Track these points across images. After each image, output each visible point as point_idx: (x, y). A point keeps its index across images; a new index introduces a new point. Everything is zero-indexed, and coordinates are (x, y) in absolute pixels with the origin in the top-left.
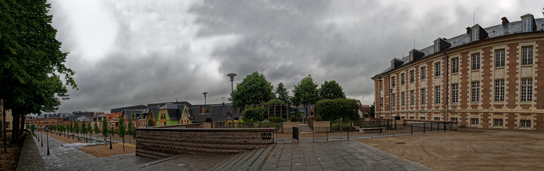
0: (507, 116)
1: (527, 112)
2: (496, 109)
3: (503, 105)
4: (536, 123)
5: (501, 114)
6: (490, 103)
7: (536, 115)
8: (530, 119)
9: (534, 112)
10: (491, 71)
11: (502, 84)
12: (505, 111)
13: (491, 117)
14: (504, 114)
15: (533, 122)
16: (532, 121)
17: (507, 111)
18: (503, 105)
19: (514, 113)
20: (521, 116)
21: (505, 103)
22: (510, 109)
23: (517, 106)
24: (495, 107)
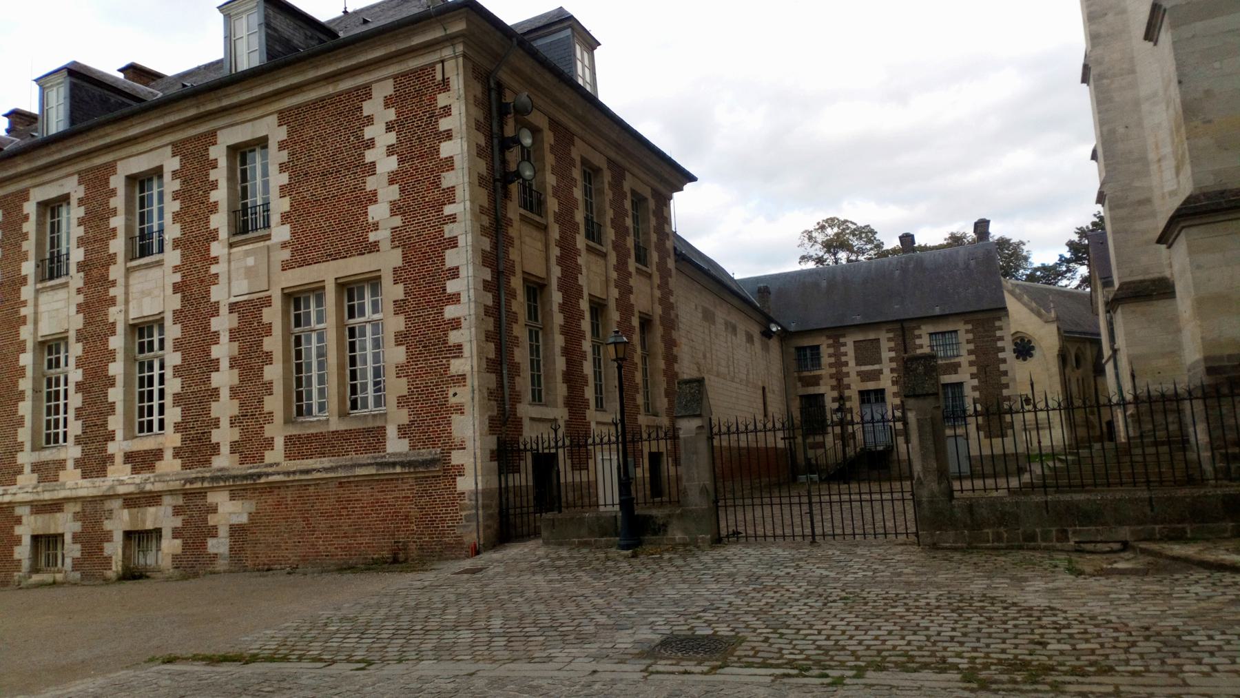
1: (47, 496)
4: (78, 546)
7: (78, 508)
8: (60, 531)
9: (74, 494)
19: (11, 505)
20: (33, 517)
23: (20, 471)
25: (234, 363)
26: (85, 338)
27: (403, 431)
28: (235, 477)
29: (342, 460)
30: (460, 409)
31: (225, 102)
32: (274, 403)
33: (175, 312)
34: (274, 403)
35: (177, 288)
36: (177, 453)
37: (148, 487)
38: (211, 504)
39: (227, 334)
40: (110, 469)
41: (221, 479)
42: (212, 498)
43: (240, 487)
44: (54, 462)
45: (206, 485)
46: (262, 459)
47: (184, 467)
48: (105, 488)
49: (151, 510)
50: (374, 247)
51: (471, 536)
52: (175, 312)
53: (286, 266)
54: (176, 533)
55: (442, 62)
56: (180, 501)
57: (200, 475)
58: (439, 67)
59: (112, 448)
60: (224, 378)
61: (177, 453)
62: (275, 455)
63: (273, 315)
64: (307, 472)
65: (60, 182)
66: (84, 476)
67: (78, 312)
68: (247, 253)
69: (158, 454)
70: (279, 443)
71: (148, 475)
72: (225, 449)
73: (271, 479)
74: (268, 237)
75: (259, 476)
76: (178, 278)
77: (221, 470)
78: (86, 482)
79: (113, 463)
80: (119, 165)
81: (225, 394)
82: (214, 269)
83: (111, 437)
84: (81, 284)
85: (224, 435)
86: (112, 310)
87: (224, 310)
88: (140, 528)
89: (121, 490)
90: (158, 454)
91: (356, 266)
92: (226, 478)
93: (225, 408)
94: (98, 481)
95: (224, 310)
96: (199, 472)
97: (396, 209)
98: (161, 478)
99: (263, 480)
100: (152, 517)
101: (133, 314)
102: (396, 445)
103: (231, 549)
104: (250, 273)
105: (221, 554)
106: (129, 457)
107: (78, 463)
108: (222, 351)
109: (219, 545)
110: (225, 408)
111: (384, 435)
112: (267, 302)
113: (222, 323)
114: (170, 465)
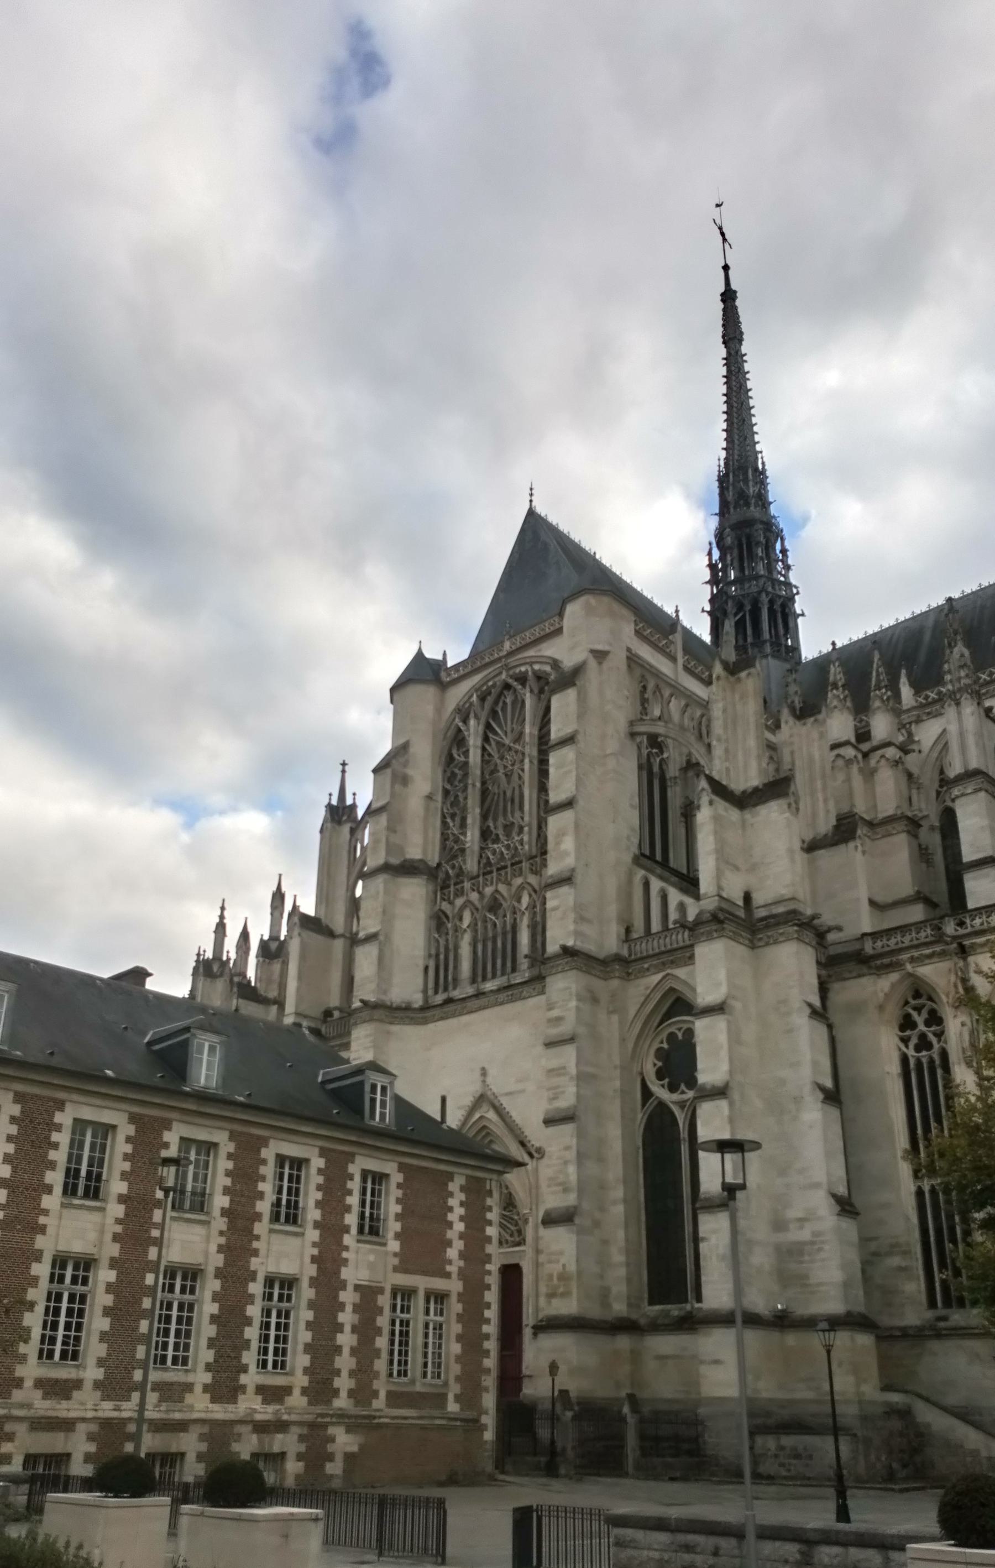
0: (91, 1437)
1: (177, 1416)
2: (48, 1404)
3: (77, 1384)
5: (67, 1425)
6: (20, 1371)
7: (206, 1429)
10: (46, 1212)
11: (74, 1280)
12: (90, 1414)
13: (16, 1443)
14: (82, 1428)
15: (194, 1459)
16: (191, 1457)
17: (100, 1414)
18: (77, 1384)
21: (92, 1373)
22: (108, 1405)
24: (39, 1393)
25: (354, 1329)
26: (225, 1277)
27: (458, 1398)
28: (356, 1417)
29: (424, 1413)
30: (487, 1390)
31: (379, 1144)
32: (381, 1365)
33: (311, 1278)
34: (381, 1365)
35: (314, 1259)
36: (304, 1391)
37: (285, 1417)
38: (330, 1435)
39: (351, 1307)
40: (241, 1397)
41: (341, 1416)
42: (331, 1430)
43: (353, 1424)
44: (179, 1384)
45: (334, 1420)
46: (370, 1404)
47: (310, 1403)
48: (242, 1414)
49: (280, 1436)
50: (448, 1275)
51: (489, 1467)
52: (311, 1278)
53: (395, 1269)
54: (300, 1457)
55: (491, 1180)
56: (305, 1431)
57: (325, 1412)
58: (488, 1182)
59: (244, 1379)
60: (346, 1339)
61: (304, 1391)
62: (380, 1403)
63: (384, 1301)
64: (406, 1418)
65: (209, 1129)
66: (213, 1400)
67: (218, 1252)
68: (371, 1251)
69: (287, 1390)
70: (382, 1394)
71: (278, 1407)
72: (344, 1394)
73: (382, 1420)
74: (385, 1245)
75: (374, 1417)
76: (315, 1251)
77: (340, 1409)
78: (216, 1407)
79: (244, 1393)
80: (272, 1143)
81: (346, 1351)
82: (345, 1255)
83: (245, 1369)
84: (224, 1228)
85: (343, 1383)
86: (253, 1260)
87: (350, 1288)
88: (266, 1450)
89: (258, 1417)
90: (287, 1390)
91: (438, 1284)
92: (349, 1417)
93: (345, 1362)
94: (230, 1407)
95: (350, 1288)
96: (323, 1409)
97: (462, 1255)
98: (290, 1411)
99: (376, 1421)
100: (279, 1442)
101: (272, 1268)
102: (453, 1407)
103: (344, 1471)
104: (371, 1266)
105: (336, 1475)
106: (260, 1389)
107: (206, 1388)
108: (347, 1317)
109: (334, 1468)
110: (345, 1362)
111: (446, 1399)
112: (381, 1291)
113: (348, 1297)
114: (297, 1400)
